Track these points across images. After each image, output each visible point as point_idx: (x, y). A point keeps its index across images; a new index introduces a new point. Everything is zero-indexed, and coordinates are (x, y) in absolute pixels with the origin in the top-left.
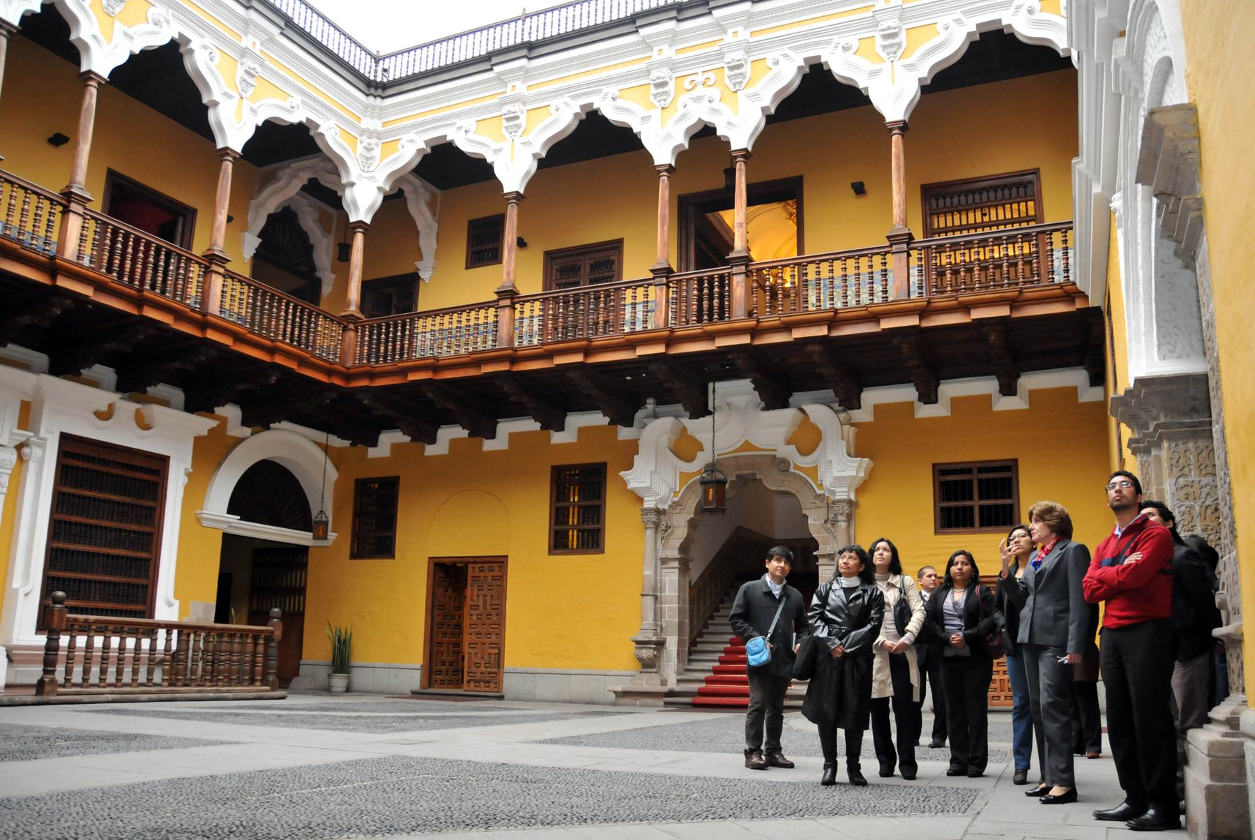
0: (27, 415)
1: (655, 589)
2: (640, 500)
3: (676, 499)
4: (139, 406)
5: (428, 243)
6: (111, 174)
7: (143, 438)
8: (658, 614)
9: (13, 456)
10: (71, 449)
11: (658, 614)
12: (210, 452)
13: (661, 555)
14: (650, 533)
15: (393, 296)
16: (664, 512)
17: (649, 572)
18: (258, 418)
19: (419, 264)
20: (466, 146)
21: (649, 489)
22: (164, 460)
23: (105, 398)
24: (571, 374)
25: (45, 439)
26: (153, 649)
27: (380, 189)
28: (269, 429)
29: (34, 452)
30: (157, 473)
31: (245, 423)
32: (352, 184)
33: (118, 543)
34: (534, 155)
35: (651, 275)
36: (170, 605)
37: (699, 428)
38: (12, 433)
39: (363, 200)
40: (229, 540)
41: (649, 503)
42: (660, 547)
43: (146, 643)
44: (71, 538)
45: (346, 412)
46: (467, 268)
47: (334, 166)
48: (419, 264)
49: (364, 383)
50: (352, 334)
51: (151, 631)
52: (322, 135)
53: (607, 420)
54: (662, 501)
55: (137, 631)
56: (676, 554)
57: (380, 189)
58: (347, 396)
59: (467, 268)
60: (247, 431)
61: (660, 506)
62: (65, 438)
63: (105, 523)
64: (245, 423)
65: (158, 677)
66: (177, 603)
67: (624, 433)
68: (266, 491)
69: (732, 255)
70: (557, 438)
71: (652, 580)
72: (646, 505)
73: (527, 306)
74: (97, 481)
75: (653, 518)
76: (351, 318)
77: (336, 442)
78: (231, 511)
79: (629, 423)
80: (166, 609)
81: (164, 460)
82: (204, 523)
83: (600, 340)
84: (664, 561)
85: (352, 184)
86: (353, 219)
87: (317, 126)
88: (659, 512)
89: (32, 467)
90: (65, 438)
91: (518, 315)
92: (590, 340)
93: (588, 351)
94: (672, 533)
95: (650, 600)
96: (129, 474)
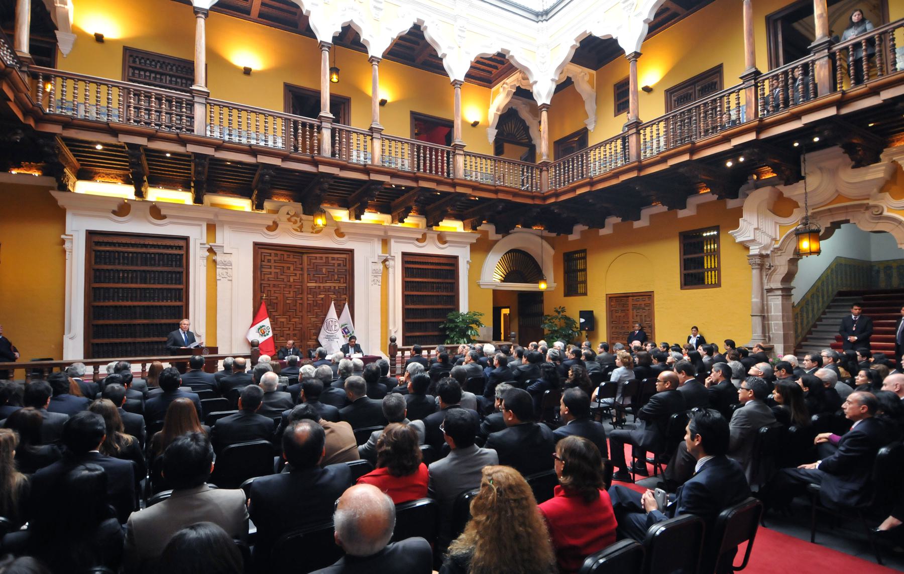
1: (762, 310)
2: (747, 249)
3: (777, 246)
5: (590, 106)
6: (412, 113)
8: (765, 329)
9: (381, 266)
11: (765, 329)
13: (766, 287)
14: (756, 272)
15: (573, 145)
16: (767, 256)
17: (756, 300)
18: (504, 229)
19: (586, 122)
20: (599, 33)
21: (753, 241)
24: (681, 170)
27: (553, 80)
28: (509, 234)
29: (390, 263)
31: (497, 232)
32: (535, 82)
33: (438, 303)
34: (645, 21)
35: (741, 82)
37: (794, 191)
41: (754, 250)
42: (765, 281)
44: (413, 303)
45: (555, 217)
46: (615, 116)
47: (525, 72)
48: (586, 122)
49: (552, 200)
52: (512, 57)
53: (715, 197)
54: (765, 248)
56: (779, 286)
57: (553, 80)
58: (546, 209)
59: (615, 116)
60: (500, 236)
61: (764, 252)
62: (404, 254)
64: (497, 232)
67: (731, 204)
68: (522, 266)
69: (813, 44)
70: (682, 214)
71: (759, 305)
72: (752, 252)
73: (648, 129)
74: (423, 273)
75: (758, 261)
76: (545, 164)
79: (735, 196)
83: (700, 142)
84: (770, 290)
85: (535, 82)
86: (539, 104)
87: (509, 52)
88: (762, 256)
89: (391, 270)
90: (404, 254)
91: (642, 137)
92: (693, 143)
93: (693, 150)
94: (775, 271)
95: (758, 320)
96: (439, 267)
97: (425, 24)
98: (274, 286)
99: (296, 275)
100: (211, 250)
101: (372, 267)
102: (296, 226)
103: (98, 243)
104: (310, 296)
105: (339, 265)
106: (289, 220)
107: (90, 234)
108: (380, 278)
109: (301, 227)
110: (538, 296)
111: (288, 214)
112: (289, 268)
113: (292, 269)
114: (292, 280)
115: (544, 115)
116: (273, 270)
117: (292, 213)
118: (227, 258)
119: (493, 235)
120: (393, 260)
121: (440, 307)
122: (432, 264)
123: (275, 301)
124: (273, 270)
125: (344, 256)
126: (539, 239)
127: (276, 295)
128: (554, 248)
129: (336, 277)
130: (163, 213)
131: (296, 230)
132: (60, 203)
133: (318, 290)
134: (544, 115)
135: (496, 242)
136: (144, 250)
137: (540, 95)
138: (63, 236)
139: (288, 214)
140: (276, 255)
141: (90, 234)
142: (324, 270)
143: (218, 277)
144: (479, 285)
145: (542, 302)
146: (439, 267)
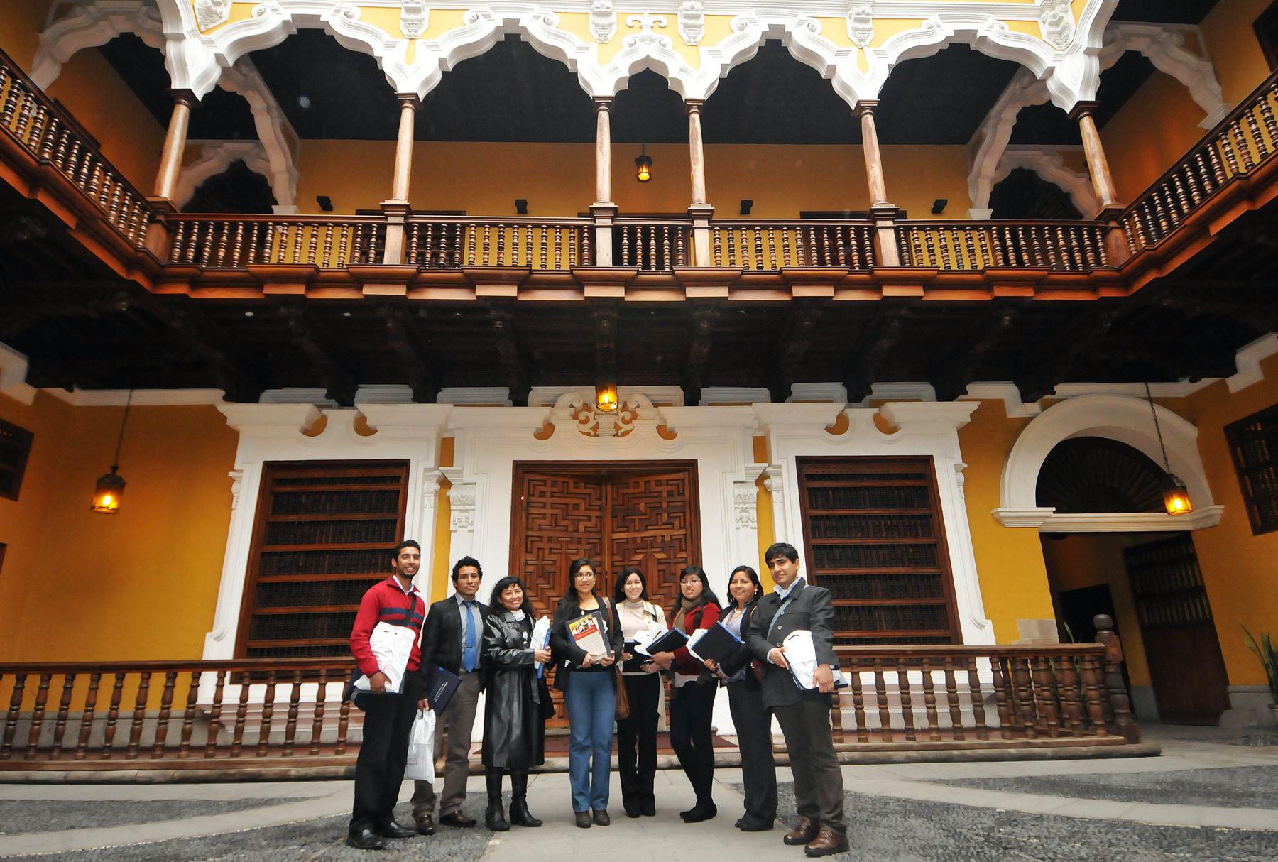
0: (761, 449)
4: (876, 410)
7: (890, 442)
9: (754, 490)
10: (809, 470)
12: (987, 443)
22: (927, 461)
23: (829, 412)
25: (780, 467)
26: (974, 683)
29: (772, 482)
30: (919, 476)
31: (1026, 397)
32: (1051, 71)
33: (895, 562)
36: (981, 627)
38: (747, 469)
39: (1072, 77)
40: (1050, 540)
43: (961, 677)
44: (835, 562)
50: (1117, 233)
51: (966, 658)
55: (938, 661)
60: (1033, 407)
62: (802, 462)
63: (871, 541)
64: (1026, 397)
65: (992, 719)
66: (989, 624)
74: (852, 497)
76: (1108, 214)
77: (1182, 389)
78: (1040, 503)
80: (976, 629)
81: (927, 461)
82: (1007, 524)
89: (776, 496)
90: (802, 462)
96: (887, 483)
97: (787, 29)
98: (550, 539)
99: (589, 519)
100: (445, 483)
101: (733, 491)
102: (587, 428)
103: (280, 482)
104: (617, 558)
105: (670, 493)
106: (575, 417)
107: (271, 469)
108: (753, 514)
109: (596, 428)
110: (1176, 546)
111: (572, 406)
112: (577, 507)
113: (582, 507)
114: (582, 528)
115: (1087, 125)
116: (549, 511)
117: (578, 405)
118: (466, 492)
119: (1017, 408)
120: (779, 474)
121: (901, 570)
122: (870, 476)
123: (551, 569)
124: (549, 511)
125: (679, 476)
126: (1146, 406)
127: (554, 557)
128: (1194, 423)
129: (665, 516)
130: (370, 423)
131: (588, 434)
132: (230, 422)
133: (631, 546)
134: (1087, 125)
135: (1026, 421)
136: (343, 488)
137: (1065, 91)
138: (231, 474)
139: (572, 406)
140: (554, 484)
141: (271, 469)
142: (642, 507)
143: (452, 527)
144: (999, 521)
145: (1192, 559)
146: (887, 483)
